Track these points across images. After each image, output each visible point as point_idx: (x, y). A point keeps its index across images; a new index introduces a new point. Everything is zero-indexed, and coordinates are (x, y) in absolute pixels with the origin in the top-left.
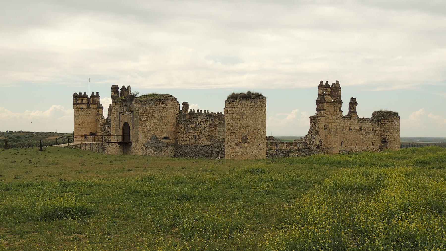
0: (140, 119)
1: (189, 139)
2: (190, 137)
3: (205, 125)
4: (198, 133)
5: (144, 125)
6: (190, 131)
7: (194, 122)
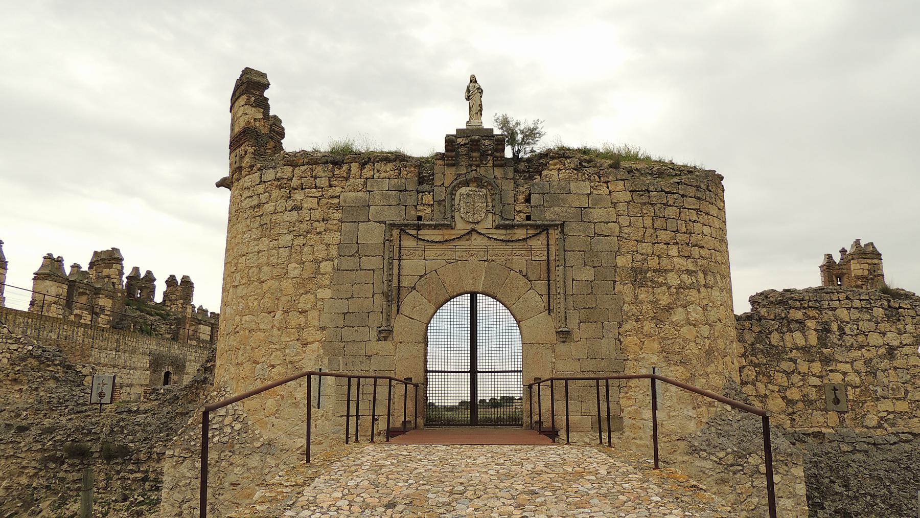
0: (638, 277)
1: (790, 402)
2: (794, 394)
3: (892, 338)
4: (846, 371)
5: (678, 315)
6: (785, 365)
7: (811, 324)
